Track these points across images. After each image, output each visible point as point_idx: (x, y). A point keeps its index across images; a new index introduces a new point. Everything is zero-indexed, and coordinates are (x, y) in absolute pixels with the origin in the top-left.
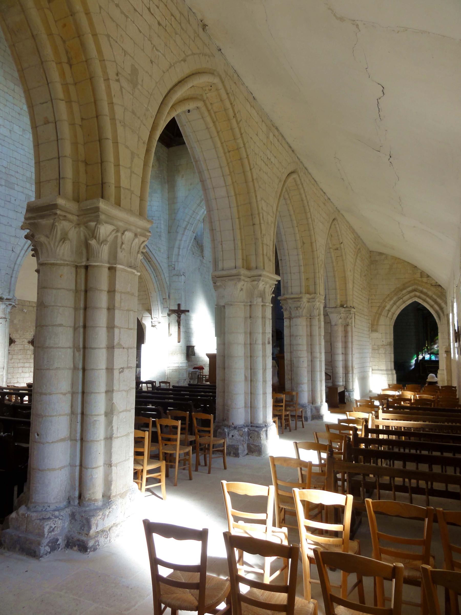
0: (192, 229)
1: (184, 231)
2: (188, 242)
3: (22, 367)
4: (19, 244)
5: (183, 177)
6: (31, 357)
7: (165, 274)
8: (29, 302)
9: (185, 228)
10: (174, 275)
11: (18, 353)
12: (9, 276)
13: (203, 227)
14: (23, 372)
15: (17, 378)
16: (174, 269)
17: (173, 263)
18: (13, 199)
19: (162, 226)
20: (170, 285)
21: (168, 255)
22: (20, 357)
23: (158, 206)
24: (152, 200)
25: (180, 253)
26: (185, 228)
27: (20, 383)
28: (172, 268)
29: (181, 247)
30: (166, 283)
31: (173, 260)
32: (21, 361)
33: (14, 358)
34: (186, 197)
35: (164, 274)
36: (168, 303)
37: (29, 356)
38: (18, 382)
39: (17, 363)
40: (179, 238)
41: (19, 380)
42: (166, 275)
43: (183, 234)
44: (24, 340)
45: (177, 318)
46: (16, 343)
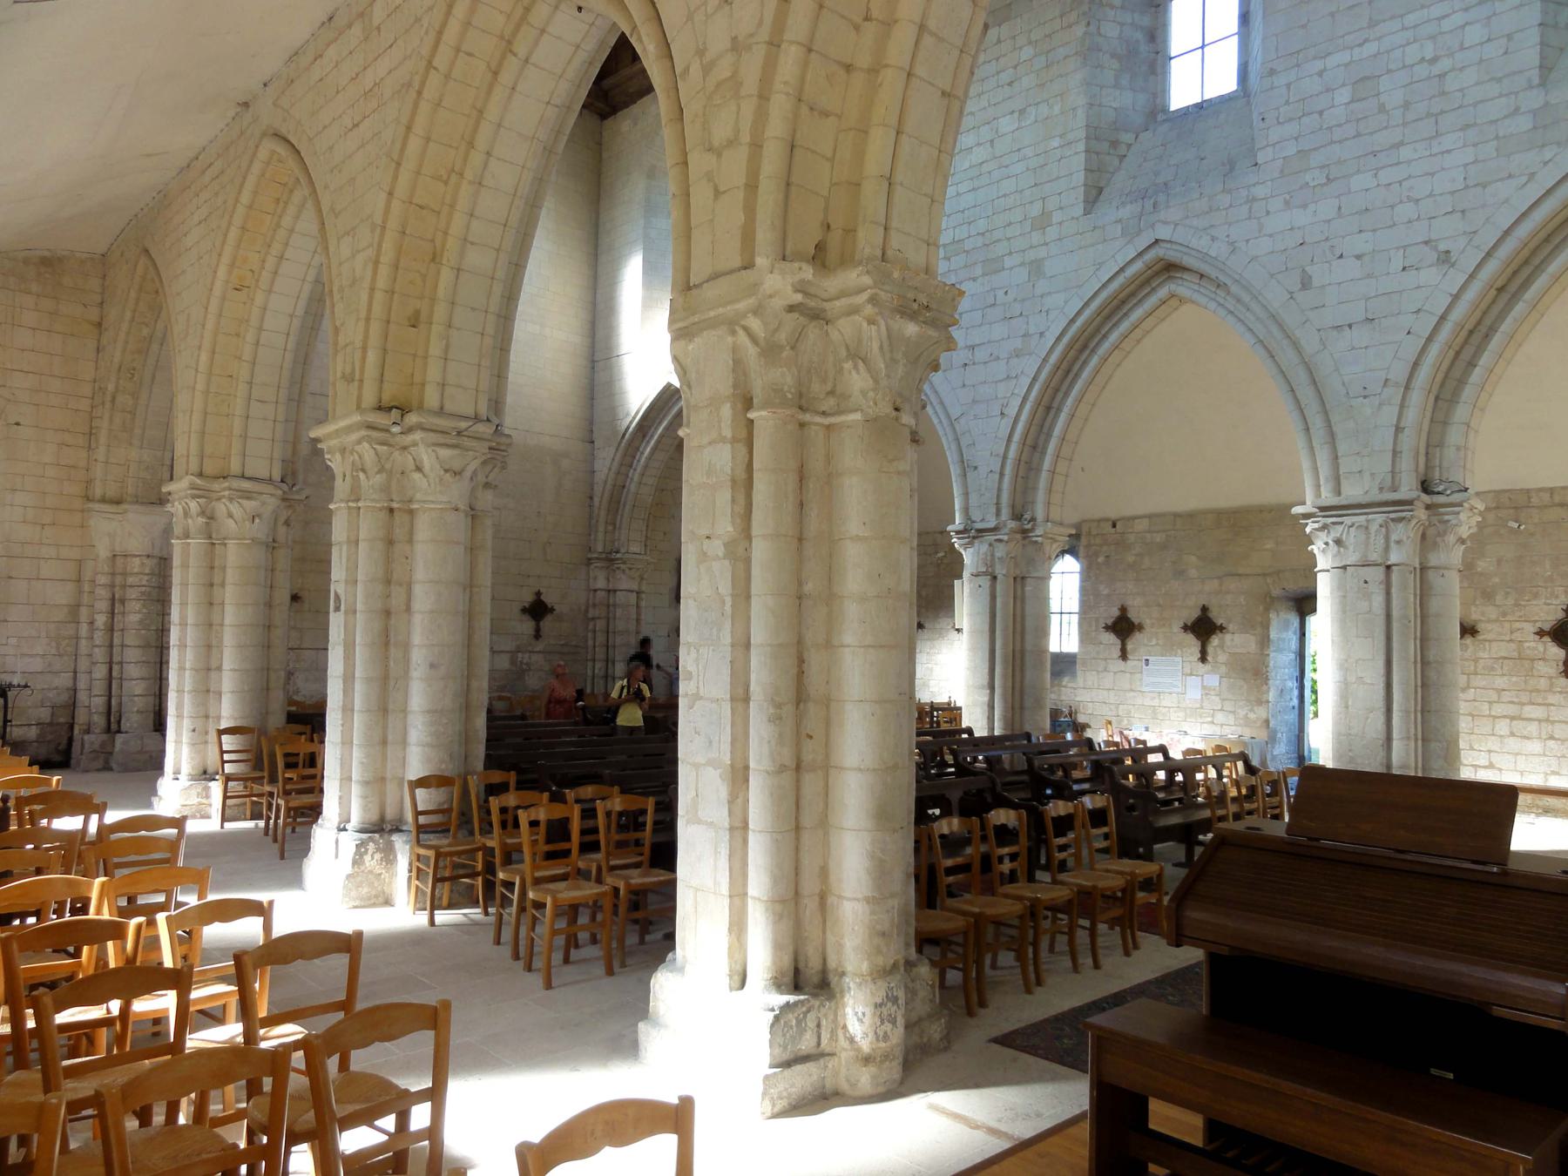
3: (1513, 718)
4: (1016, 391)
6: (1552, 685)
8: (1552, 491)
11: (1493, 669)
12: (997, 476)
14: (1512, 734)
15: (1490, 751)
18: (1000, 293)
22: (1500, 682)
27: (1500, 770)
32: (1506, 696)
33: (1473, 683)
37: (1543, 683)
38: (1491, 766)
39: (1490, 702)
41: (1495, 758)
44: (1517, 625)
46: (1480, 637)
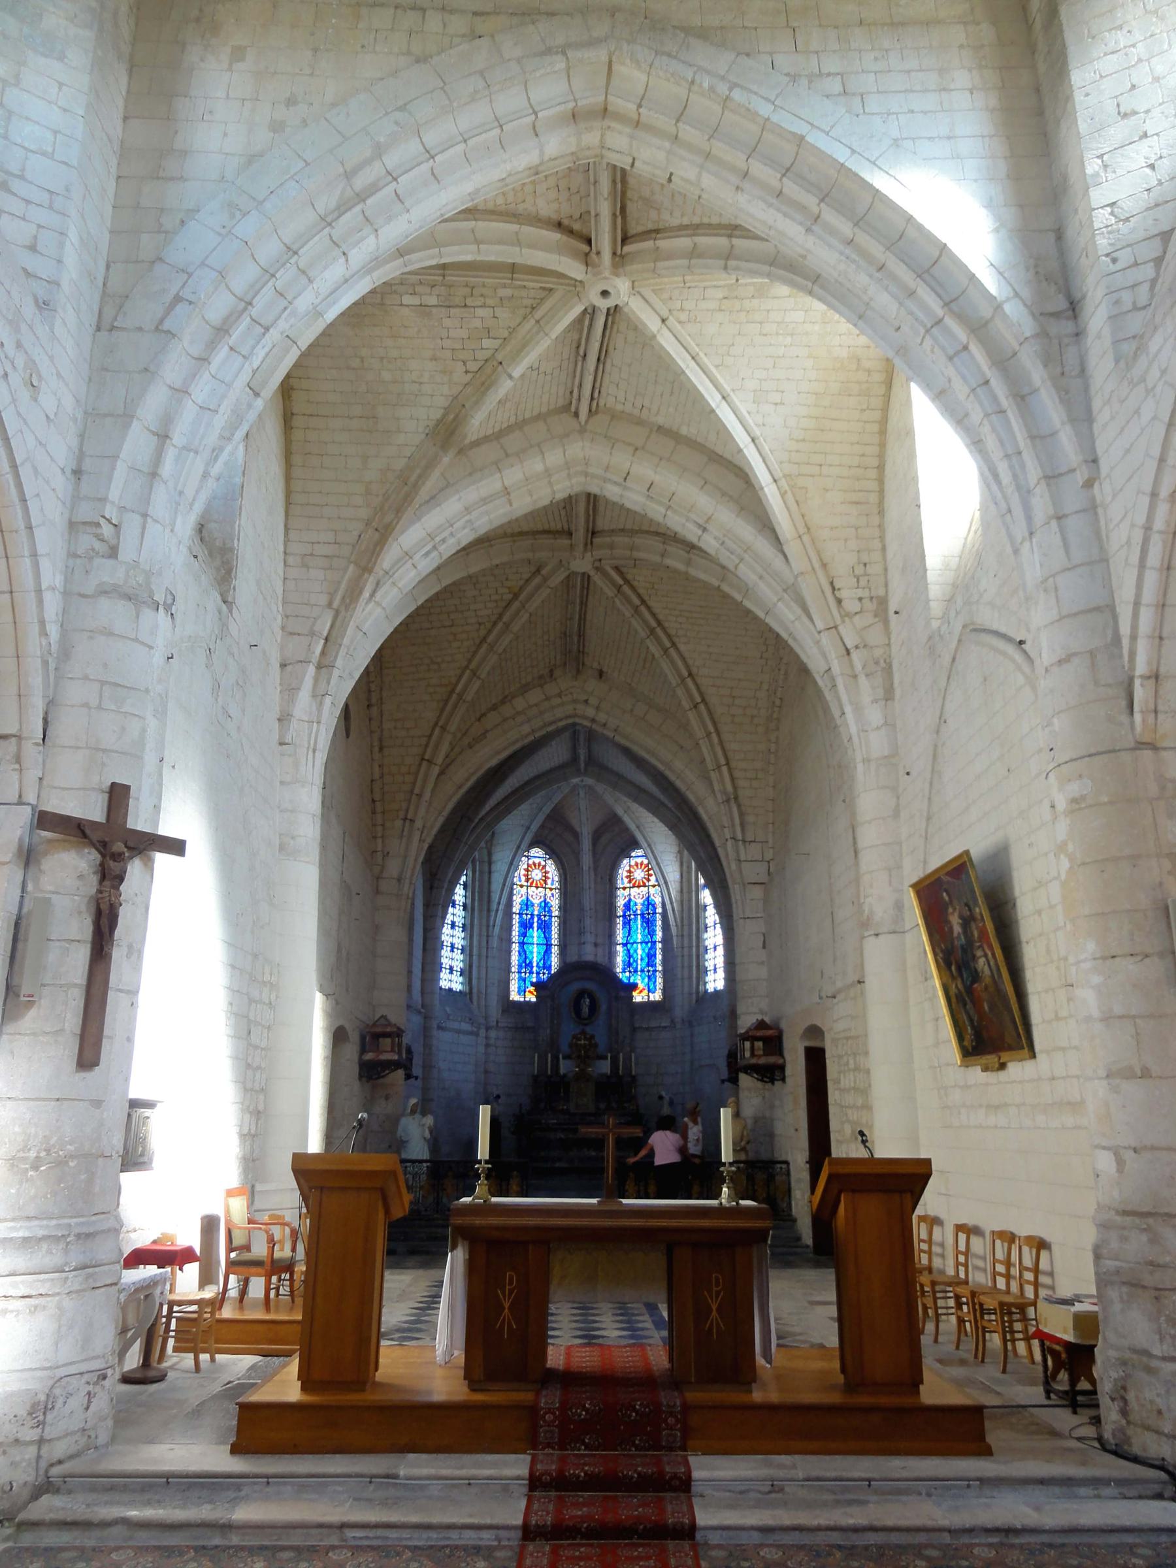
0: (260, 353)
1: (212, 345)
2: (220, 421)
5: (238, 54)
7: (45, 565)
9: (222, 330)
10: (106, 592)
13: (240, 461)
16: (113, 552)
17: (110, 512)
19: (71, 258)
20: (66, 652)
21: (81, 456)
23: (55, 132)
24: (17, 76)
25: (167, 467)
26: (222, 330)
28: (97, 545)
29: (178, 437)
30: (44, 633)
31: (114, 494)
34: (251, 159)
35: (34, 555)
36: (32, 774)
40: (173, 369)
42: (52, 576)
43: (204, 360)
45: (92, 883)
